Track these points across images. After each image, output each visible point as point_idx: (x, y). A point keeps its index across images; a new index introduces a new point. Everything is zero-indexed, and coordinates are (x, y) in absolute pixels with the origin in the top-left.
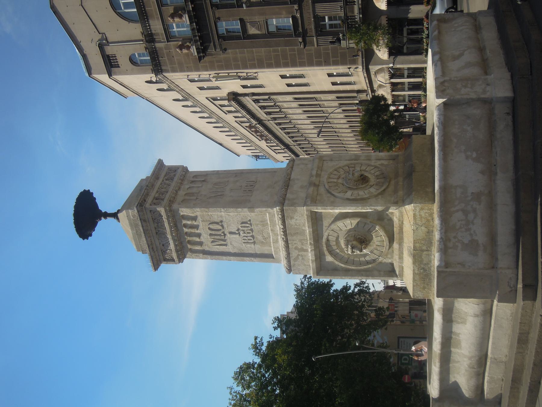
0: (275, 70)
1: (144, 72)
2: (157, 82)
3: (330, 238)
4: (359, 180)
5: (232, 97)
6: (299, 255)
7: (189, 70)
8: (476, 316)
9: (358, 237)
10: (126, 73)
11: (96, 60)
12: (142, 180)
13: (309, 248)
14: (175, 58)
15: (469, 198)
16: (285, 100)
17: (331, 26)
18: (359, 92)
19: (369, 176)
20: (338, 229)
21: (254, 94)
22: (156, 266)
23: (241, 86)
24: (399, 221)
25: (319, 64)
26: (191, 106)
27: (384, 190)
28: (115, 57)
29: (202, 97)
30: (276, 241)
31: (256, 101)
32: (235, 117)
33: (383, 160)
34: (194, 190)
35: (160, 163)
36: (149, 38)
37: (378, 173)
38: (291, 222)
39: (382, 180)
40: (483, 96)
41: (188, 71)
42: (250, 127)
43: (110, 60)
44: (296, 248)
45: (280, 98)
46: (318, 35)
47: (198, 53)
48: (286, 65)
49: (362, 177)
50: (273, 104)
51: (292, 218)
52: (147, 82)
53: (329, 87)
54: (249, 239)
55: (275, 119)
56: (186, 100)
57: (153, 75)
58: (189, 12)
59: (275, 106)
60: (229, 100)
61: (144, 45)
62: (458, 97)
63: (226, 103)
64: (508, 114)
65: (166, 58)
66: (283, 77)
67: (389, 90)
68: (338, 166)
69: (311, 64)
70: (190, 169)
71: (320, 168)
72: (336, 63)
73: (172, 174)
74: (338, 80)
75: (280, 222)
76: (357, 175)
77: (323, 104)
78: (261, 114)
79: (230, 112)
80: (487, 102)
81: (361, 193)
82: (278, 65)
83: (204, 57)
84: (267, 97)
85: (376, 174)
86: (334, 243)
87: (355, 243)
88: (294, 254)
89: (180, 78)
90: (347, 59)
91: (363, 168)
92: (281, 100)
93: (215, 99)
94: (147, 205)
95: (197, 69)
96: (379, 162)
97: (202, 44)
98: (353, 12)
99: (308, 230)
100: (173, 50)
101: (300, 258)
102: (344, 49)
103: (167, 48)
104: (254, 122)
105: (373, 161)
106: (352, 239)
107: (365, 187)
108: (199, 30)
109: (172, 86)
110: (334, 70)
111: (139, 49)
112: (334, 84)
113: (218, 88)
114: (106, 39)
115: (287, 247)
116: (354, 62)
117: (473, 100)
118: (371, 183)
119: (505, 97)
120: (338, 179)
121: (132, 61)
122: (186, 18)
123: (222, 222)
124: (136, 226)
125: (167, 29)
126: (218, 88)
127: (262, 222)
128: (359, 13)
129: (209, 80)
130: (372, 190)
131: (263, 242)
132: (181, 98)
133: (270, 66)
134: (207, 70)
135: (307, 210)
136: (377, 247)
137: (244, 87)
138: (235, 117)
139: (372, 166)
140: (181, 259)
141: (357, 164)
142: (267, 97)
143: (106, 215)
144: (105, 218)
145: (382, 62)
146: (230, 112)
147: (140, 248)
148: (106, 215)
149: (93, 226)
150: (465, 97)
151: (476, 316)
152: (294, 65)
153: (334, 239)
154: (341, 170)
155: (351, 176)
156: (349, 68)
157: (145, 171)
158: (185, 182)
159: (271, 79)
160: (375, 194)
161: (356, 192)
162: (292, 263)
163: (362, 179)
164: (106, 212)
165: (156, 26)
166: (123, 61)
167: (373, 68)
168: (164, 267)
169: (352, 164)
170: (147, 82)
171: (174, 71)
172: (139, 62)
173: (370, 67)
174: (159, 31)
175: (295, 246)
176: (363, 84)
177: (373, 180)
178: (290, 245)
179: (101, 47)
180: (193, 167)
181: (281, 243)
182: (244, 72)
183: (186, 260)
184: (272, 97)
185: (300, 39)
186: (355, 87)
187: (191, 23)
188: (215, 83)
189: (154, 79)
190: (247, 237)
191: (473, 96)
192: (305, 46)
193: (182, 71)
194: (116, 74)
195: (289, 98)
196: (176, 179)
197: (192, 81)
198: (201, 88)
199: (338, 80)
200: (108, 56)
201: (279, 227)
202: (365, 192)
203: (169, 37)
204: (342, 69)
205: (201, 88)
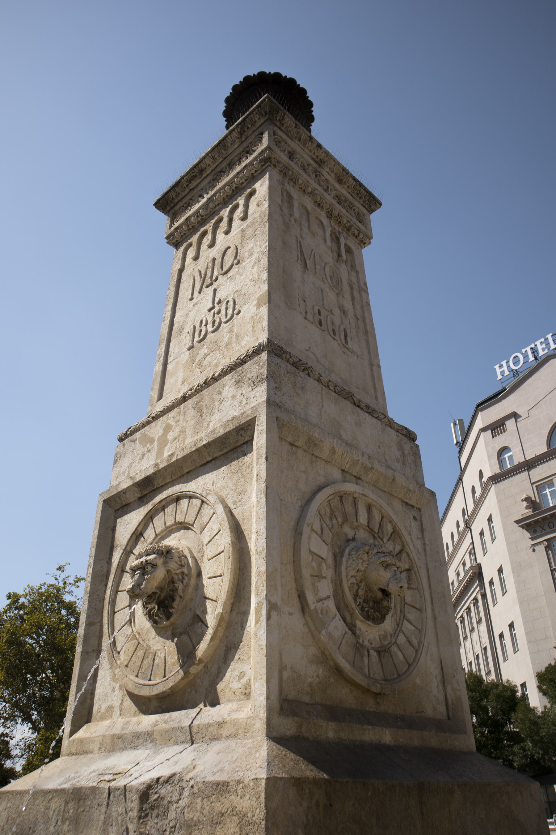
3: (184, 503)
6: (152, 441)
9: (180, 586)
10: (487, 445)
19: (388, 624)
20: (206, 520)
21: (484, 596)
23: (492, 579)
24: (220, 724)
28: (504, 432)
35: (372, 203)
54: (201, 331)
70: (366, 252)
79: (458, 574)
91: (412, 615)
106: (173, 565)
111: (517, 456)
121: (503, 450)
123: (238, 263)
127: (237, 337)
135: (255, 409)
136: (151, 657)
146: (458, 574)
153: (180, 518)
154: (398, 548)
162: (138, 435)
166: (501, 441)
172: (502, 458)
175: (173, 423)
179: (515, 415)
180: (369, 255)
190: (206, 325)
200: (503, 424)
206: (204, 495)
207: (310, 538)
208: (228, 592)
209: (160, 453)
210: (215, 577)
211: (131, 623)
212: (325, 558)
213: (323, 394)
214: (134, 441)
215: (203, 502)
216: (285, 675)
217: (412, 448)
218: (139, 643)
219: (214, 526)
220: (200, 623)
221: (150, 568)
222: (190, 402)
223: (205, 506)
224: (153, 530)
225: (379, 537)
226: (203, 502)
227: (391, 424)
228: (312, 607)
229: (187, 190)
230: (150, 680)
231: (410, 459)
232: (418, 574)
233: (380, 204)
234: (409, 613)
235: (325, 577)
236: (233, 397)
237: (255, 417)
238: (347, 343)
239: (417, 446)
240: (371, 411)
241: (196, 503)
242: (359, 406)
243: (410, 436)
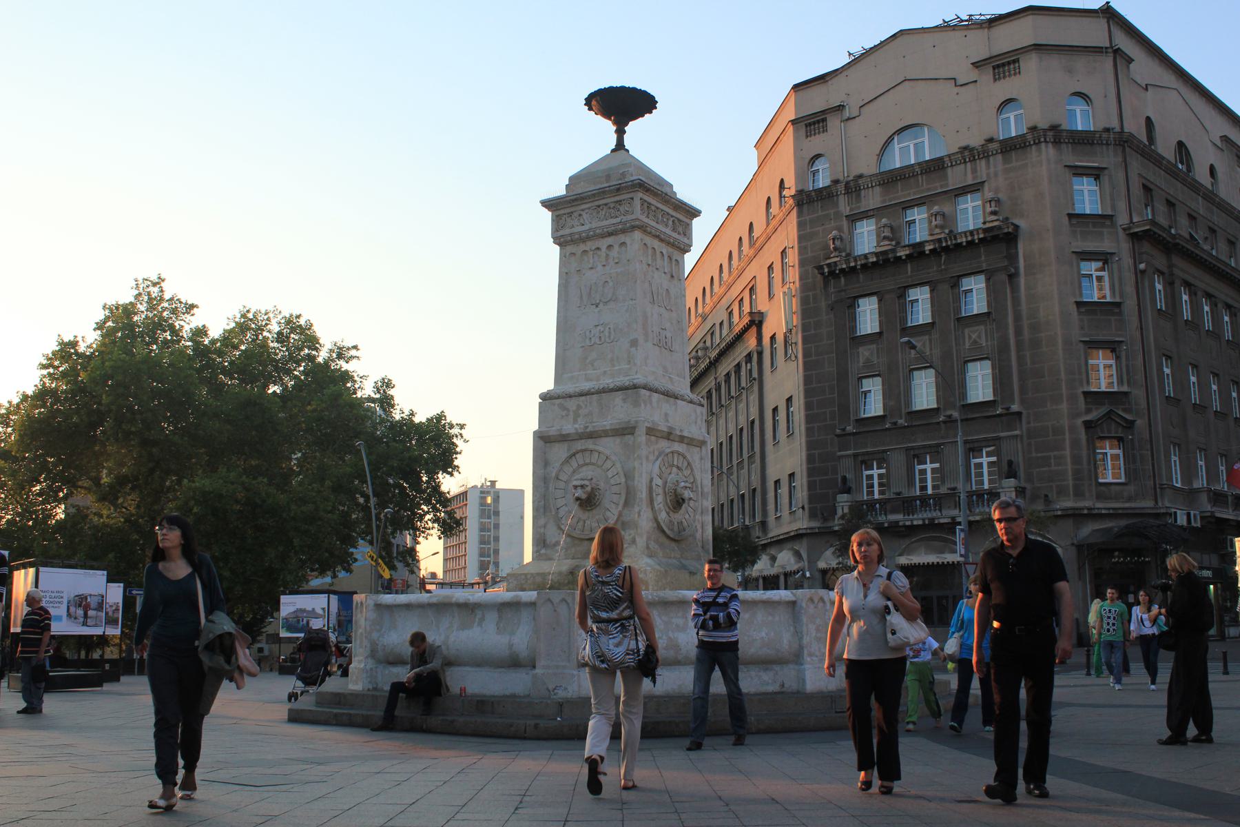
0: (802, 388)
1: (799, 176)
2: (781, 196)
5: (757, 319)
6: (568, 410)
7: (802, 250)
8: (511, 646)
10: (798, 149)
11: (818, 101)
12: (671, 186)
13: (579, 426)
14: (820, 229)
15: (671, 635)
16: (751, 405)
17: (870, 477)
18: (764, 524)
21: (760, 354)
22: (548, 204)
25: (810, 459)
26: (740, 251)
27: (663, 532)
29: (757, 269)
30: (588, 379)
31: (749, 357)
32: (721, 324)
34: (659, 262)
36: (853, 187)
37: (685, 524)
38: (618, 398)
39: (676, 529)
40: (806, 652)
41: (800, 248)
42: (706, 349)
43: (818, 122)
44: (579, 407)
45: (754, 397)
46: (855, 456)
47: (829, 265)
48: (808, 406)
50: (743, 384)
51: (624, 400)
52: (782, 181)
53: (773, 473)
55: (718, 388)
56: (751, 245)
57: (793, 192)
58: (893, 251)
59: (740, 388)
60: (751, 313)
61: (841, 178)
62: (805, 620)
63: (746, 309)
64: (783, 686)
65: (820, 213)
66: (789, 400)
67: (766, 573)
69: (811, 445)
72: (811, 486)
73: (680, 229)
74: (784, 491)
75: (618, 384)
76: (687, 494)
77: (742, 468)
78: (726, 366)
80: (796, 658)
81: (659, 499)
82: (808, 393)
83: (822, 274)
84: (755, 375)
87: (589, 489)
88: (572, 404)
89: (788, 234)
90: (820, 505)
92: (751, 398)
93: (752, 290)
94: (640, 195)
95: (802, 263)
96: (699, 527)
97: (842, 270)
98: (894, 511)
99: (607, 423)
100: (833, 224)
101: (564, 413)
102: (835, 499)
103: (838, 215)
104: (713, 354)
108: (864, 266)
109: (774, 223)
110: (801, 482)
112: (777, 482)
113: (771, 296)
114: (849, 119)
115: (581, 394)
116: (813, 515)
117: (801, 639)
119: (804, 681)
120: (678, 467)
122: (886, 246)
124: (608, 177)
125: (865, 215)
126: (771, 296)
128: (890, 523)
129: (784, 282)
130: (663, 516)
131: (586, 358)
132: (756, 234)
133: (807, 380)
134: (801, 279)
137: (773, 338)
138: (721, 324)
140: (559, 240)
142: (755, 375)
143: (620, 133)
144: (616, 131)
145: (812, 562)
146: (731, 313)
147: (574, 180)
148: (620, 133)
149: (606, 114)
150: (805, 628)
151: (511, 646)
152: (809, 419)
155: (683, 484)
156: (803, 508)
157: (684, 193)
158: (671, 250)
159: (785, 381)
161: (660, 491)
162: (557, 401)
164: (625, 132)
165: (873, 199)
166: (817, 143)
167: (802, 547)
168: (547, 215)
170: (782, 181)
171: (801, 225)
173: (805, 541)
174: (863, 202)
176: (775, 531)
177: (677, 517)
179: (840, 108)
181: (586, 386)
182: (798, 338)
183: (557, 248)
184: (756, 388)
185: (850, 429)
186: (771, 519)
187: (876, 254)
188: (779, 292)
189: (785, 193)
191: (806, 640)
192: (838, 436)
193: (801, 238)
194: (796, 131)
195: (754, 414)
196: (675, 235)
197: (783, 252)
198: (770, 268)
199: (784, 491)
200: (824, 120)
201: (608, 382)
203: (854, 218)
204: (802, 495)
205: (770, 268)
209: (575, 421)
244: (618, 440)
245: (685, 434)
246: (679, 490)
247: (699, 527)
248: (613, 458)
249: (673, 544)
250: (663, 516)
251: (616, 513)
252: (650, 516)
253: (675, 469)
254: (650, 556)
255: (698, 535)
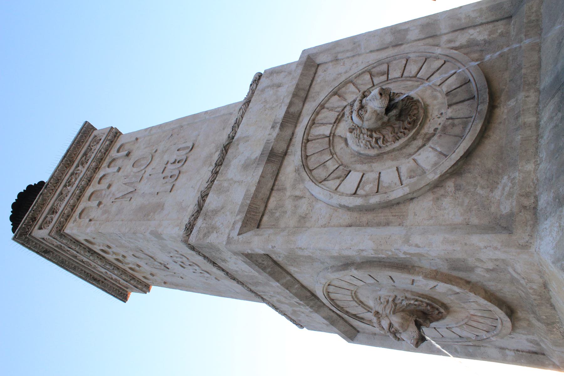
4: (384, 125)
27: (468, 155)
33: (475, 26)
37: (452, 82)
39: (462, 110)
49: (394, 112)
68: (343, 78)
71: (302, 94)
81: (393, 174)
85: (445, 88)
86: (354, 304)
87: (396, 320)
105: (445, 38)
107: (406, 145)
118: (428, 129)
120: (338, 121)
130: (427, 157)
139: (437, 58)
141: (394, 58)
160: (432, 177)
162: (293, 318)
163: (399, 117)
169: (380, 63)
178: (264, 297)
202: (406, 165)
206: (323, 286)
207: (342, 194)
208: (402, 273)
210: (392, 278)
211: (450, 328)
212: (362, 174)
213: (222, 179)
214: (300, 321)
215: (329, 285)
216: (475, 221)
217: (267, 77)
218: (466, 323)
219: (348, 278)
220: (436, 288)
221: (393, 329)
222: (253, 288)
223: (332, 283)
224: (366, 314)
225: (343, 110)
226: (329, 285)
227: (248, 102)
228: (407, 190)
229: (106, 282)
230: (497, 319)
231: (277, 79)
232: (375, 65)
233: (86, 122)
234: (411, 72)
235: (380, 173)
236: (236, 264)
237: (243, 254)
238: (188, 147)
239: (265, 71)
240: (237, 124)
241: (331, 289)
242: (233, 138)
243: (258, 78)
244: (292, 269)
245: (281, 113)
246: (366, 125)
247: (462, 39)
248: (323, 281)
249: (502, 112)
250: (429, 159)
251: (432, 283)
252: (426, 203)
253: (343, 129)
254: (534, 214)
255: (479, 35)
